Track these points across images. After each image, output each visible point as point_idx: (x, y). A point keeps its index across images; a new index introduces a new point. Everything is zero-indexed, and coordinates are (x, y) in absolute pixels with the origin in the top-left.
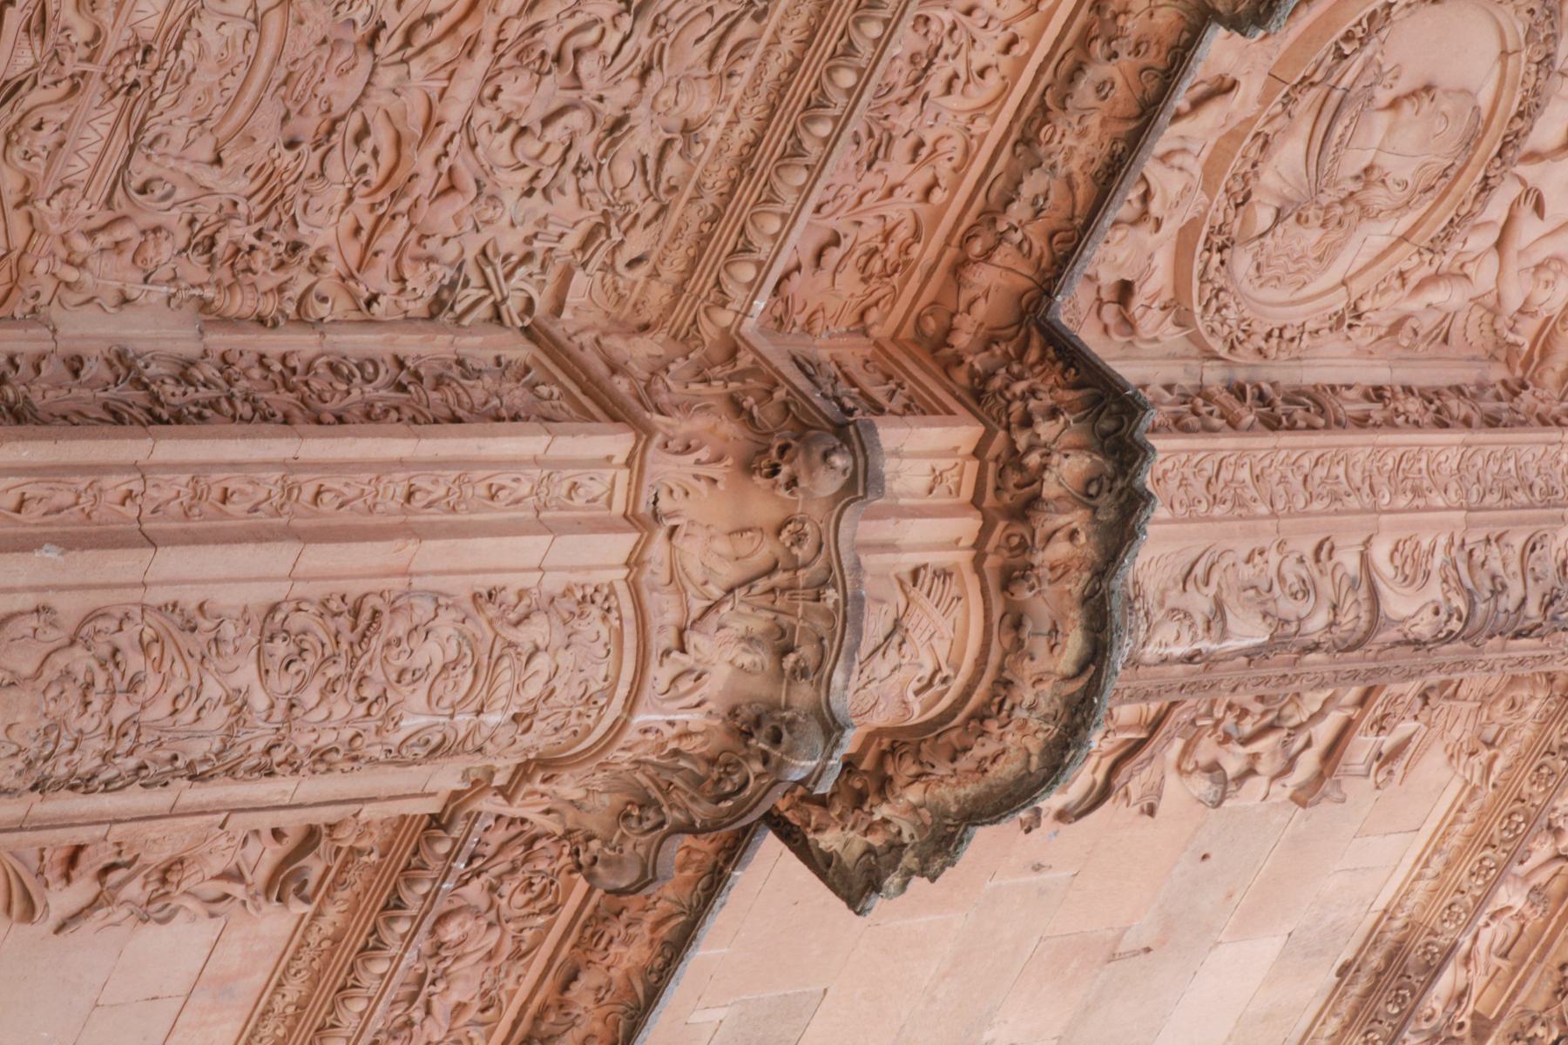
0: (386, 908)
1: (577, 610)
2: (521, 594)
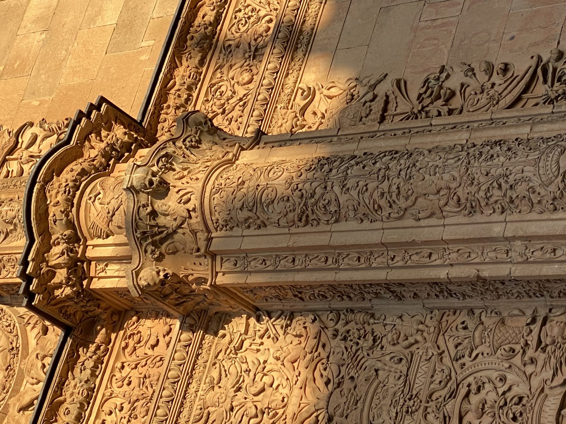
2: (249, 227)
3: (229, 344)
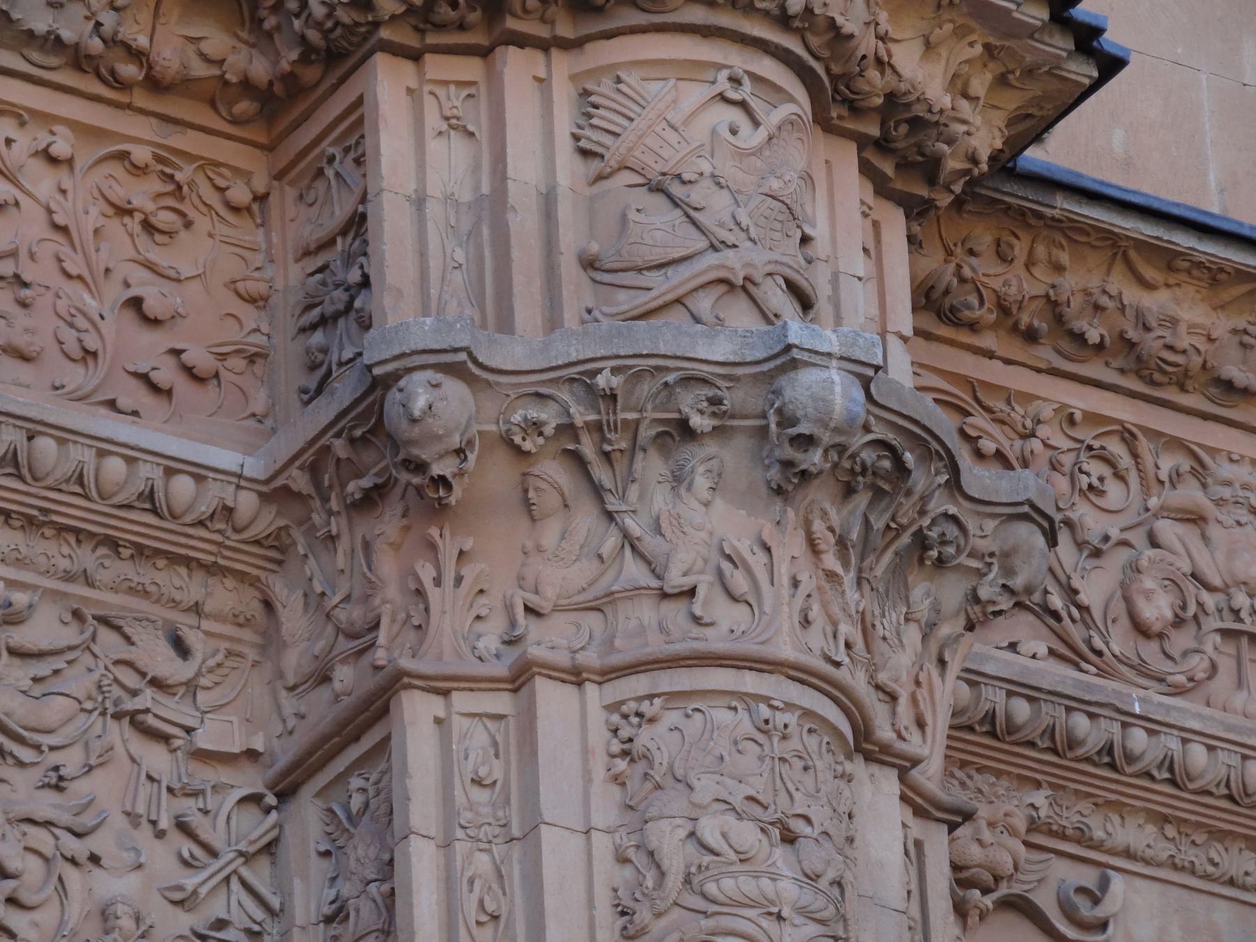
0: (1112, 766)
1: (641, 767)
3: (156, 683)
